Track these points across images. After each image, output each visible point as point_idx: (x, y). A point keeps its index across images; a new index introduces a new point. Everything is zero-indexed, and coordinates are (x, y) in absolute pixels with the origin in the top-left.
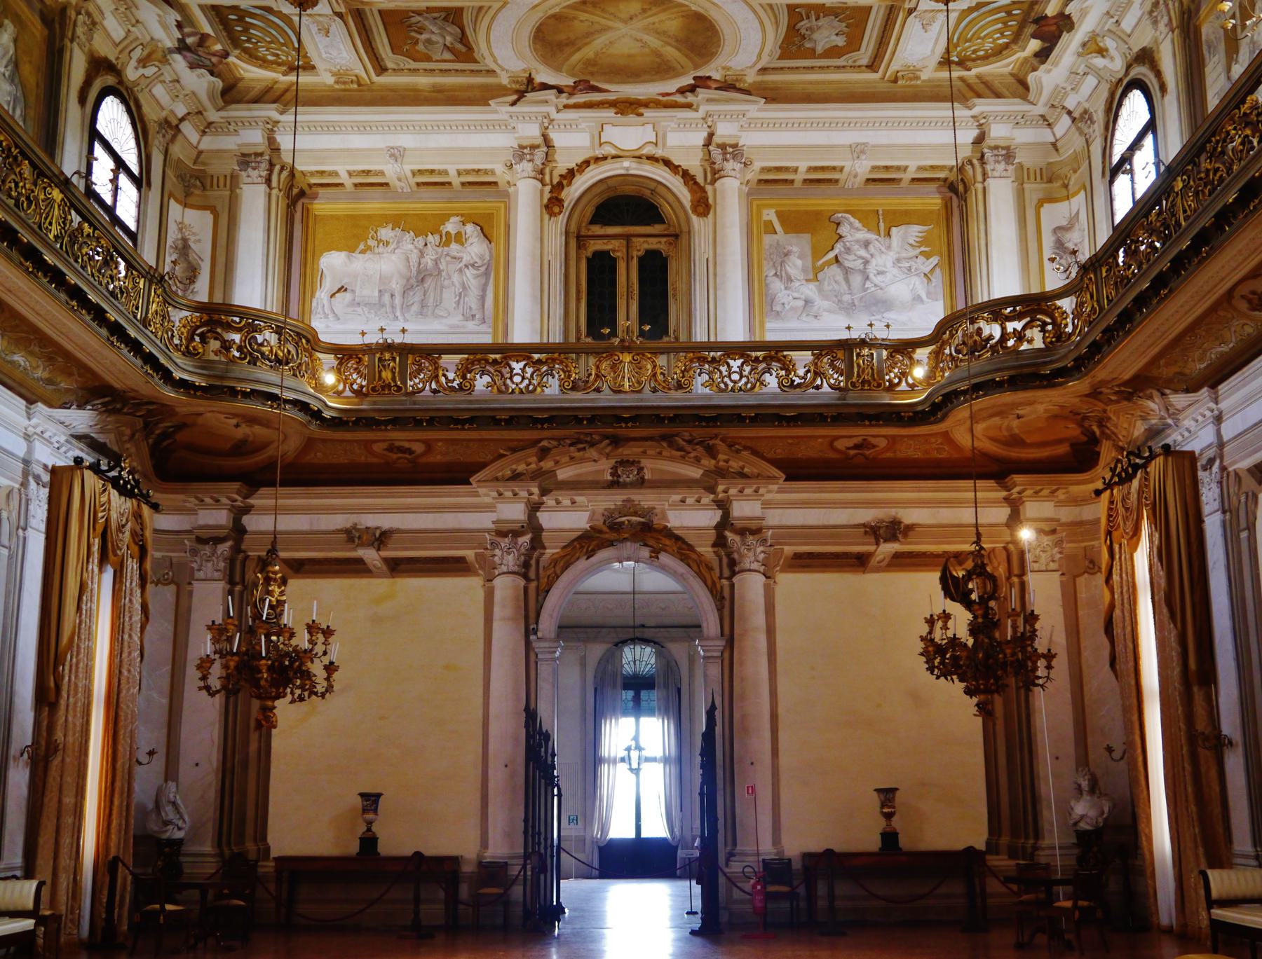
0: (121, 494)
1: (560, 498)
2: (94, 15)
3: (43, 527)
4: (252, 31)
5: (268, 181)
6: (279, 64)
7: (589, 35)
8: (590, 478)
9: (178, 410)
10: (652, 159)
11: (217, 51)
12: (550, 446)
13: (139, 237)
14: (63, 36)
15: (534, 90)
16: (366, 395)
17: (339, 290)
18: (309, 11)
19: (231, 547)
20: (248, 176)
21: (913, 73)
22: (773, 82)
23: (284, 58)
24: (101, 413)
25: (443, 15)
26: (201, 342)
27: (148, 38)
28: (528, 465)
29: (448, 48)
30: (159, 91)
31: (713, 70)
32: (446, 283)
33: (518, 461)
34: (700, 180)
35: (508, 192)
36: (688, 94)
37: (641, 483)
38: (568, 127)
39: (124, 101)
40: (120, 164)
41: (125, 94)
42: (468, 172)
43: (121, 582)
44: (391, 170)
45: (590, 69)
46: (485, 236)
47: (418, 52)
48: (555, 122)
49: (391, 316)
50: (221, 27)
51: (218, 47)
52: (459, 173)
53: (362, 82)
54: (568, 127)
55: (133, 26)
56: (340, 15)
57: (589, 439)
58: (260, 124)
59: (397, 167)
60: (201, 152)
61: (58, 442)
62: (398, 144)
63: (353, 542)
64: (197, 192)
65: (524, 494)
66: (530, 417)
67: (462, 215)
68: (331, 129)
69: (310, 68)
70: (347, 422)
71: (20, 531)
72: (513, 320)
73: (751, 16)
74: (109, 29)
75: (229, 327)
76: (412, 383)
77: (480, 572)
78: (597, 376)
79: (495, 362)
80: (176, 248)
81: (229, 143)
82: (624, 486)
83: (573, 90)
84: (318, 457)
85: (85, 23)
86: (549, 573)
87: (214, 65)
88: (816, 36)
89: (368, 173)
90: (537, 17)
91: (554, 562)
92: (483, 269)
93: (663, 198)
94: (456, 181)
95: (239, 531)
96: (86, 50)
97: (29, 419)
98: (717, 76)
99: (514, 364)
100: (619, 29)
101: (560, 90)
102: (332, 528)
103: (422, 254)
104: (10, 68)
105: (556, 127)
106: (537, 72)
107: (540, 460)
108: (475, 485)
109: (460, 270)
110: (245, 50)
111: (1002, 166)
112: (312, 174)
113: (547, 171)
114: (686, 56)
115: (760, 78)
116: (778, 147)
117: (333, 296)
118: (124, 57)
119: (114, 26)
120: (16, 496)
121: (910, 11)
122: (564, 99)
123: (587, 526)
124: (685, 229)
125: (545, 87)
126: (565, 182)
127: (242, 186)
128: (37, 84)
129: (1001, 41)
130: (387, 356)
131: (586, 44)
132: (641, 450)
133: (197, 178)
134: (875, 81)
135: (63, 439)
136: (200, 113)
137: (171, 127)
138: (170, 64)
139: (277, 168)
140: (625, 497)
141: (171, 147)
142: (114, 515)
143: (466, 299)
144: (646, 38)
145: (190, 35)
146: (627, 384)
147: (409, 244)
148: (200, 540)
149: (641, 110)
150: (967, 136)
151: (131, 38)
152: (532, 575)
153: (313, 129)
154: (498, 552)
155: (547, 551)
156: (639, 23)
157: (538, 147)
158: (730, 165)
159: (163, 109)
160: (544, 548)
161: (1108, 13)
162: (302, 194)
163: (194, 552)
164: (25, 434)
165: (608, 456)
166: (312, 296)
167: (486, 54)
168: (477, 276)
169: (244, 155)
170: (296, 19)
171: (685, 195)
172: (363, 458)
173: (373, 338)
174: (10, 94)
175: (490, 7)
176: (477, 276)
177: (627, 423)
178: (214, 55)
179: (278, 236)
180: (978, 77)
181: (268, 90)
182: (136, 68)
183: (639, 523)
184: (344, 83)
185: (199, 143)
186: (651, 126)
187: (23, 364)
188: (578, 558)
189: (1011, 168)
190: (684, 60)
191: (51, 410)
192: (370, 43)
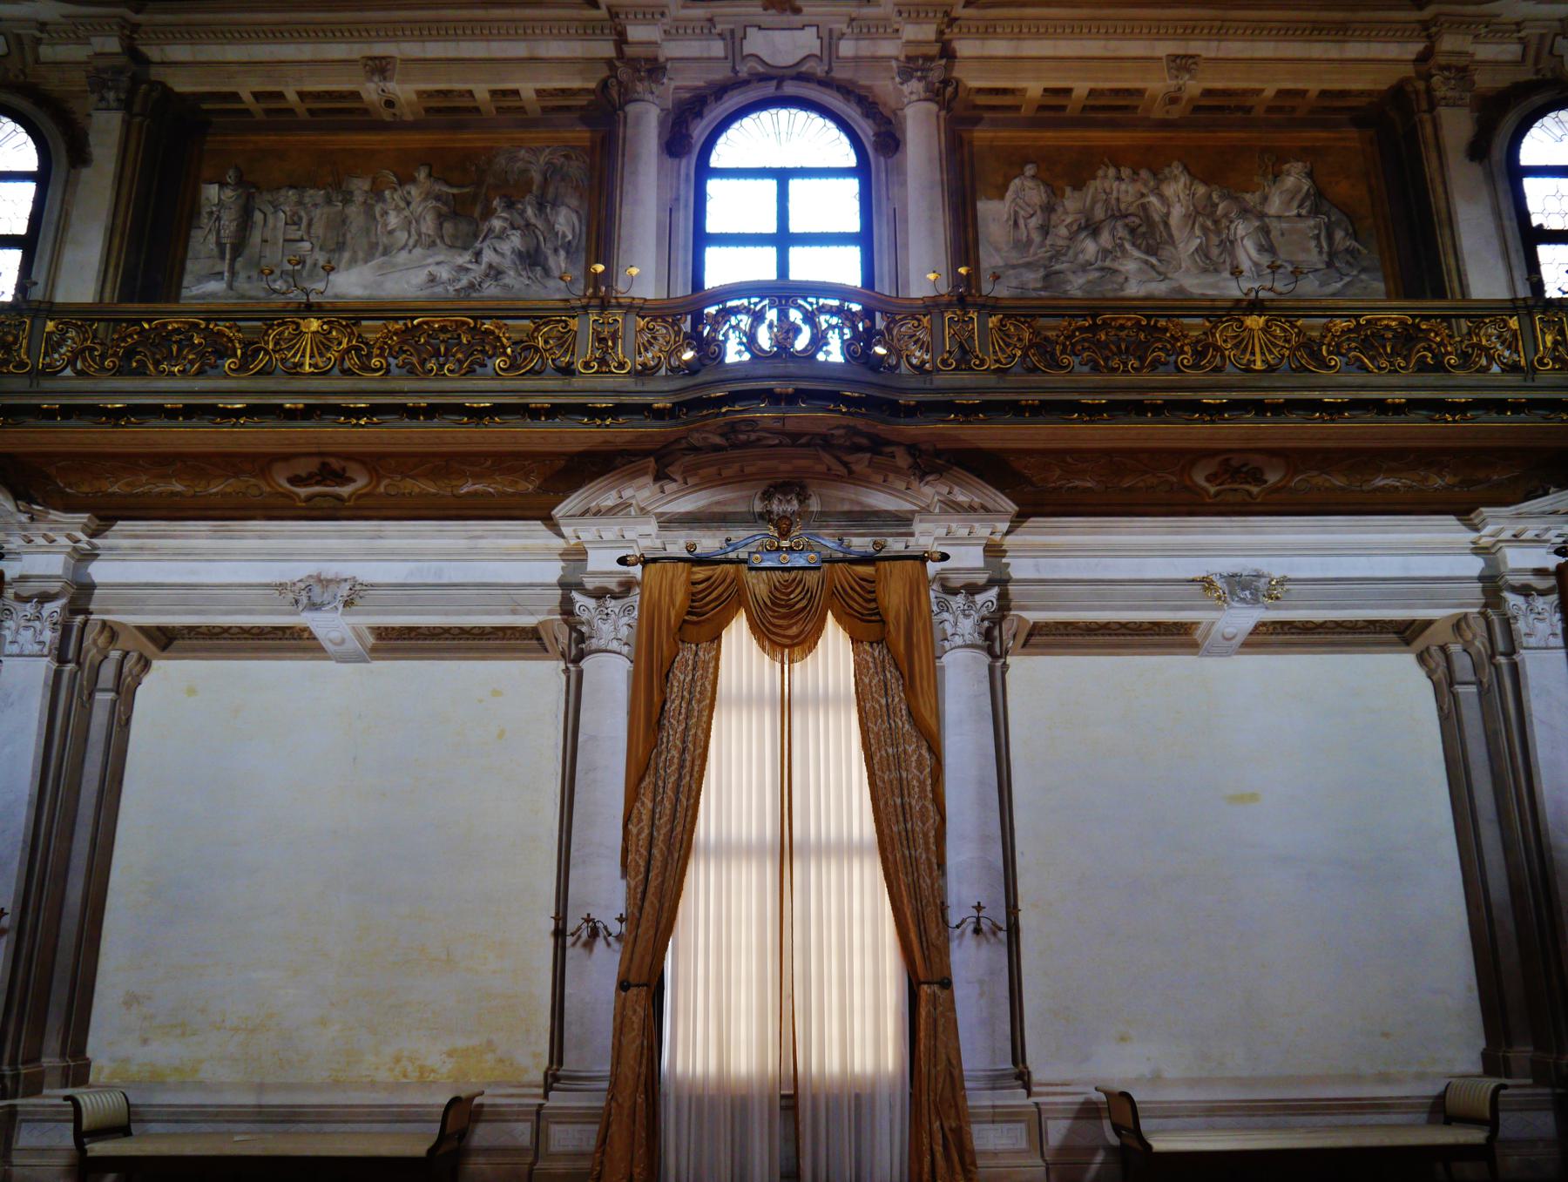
27: (1557, 24)
55: (1519, 31)
71: (1502, 660)
97: (1477, 530)
104: (1308, 203)
120: (1479, 627)
187: (1398, 484)
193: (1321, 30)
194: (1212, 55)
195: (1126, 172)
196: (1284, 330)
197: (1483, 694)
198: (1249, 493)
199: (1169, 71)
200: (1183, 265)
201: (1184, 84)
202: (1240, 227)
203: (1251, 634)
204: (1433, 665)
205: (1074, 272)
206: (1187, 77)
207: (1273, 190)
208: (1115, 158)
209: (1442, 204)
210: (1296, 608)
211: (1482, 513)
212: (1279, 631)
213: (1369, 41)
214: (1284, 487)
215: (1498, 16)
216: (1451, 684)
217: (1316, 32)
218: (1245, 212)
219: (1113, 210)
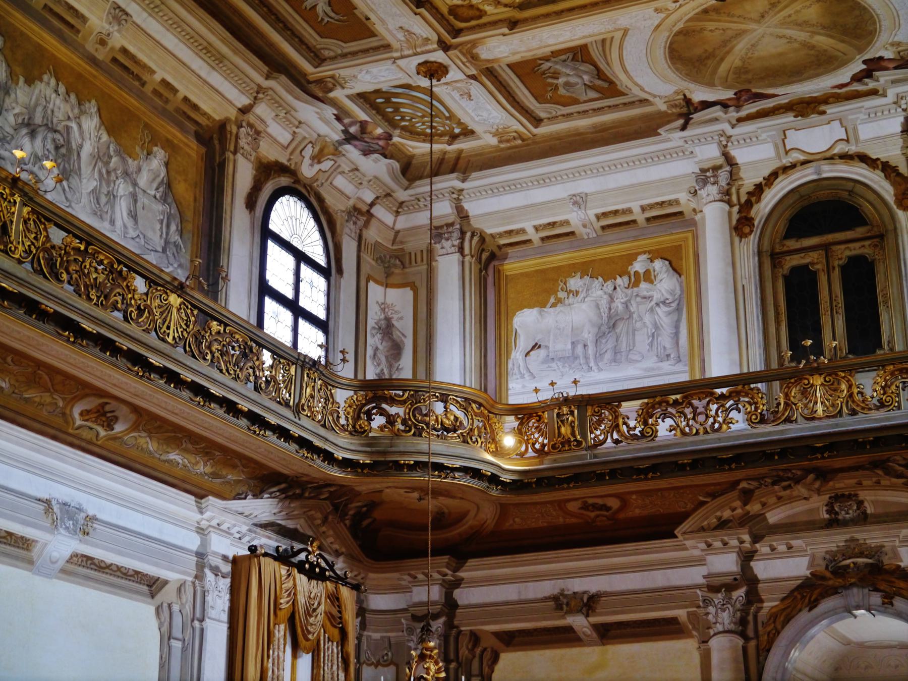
0: (310, 578)
1: (774, 544)
2: (256, 125)
3: (225, 617)
4: (402, 110)
5: (461, 249)
6: (441, 135)
7: (726, 44)
8: (804, 518)
9: (357, 489)
10: (846, 157)
11: (380, 135)
12: (752, 487)
13: (331, 324)
14: (224, 150)
15: (697, 110)
16: (547, 454)
17: (533, 348)
18: (443, 80)
19: (445, 623)
20: (442, 248)
23: (442, 129)
24: (281, 500)
26: (367, 420)
27: (315, 136)
28: (733, 510)
29: (589, 87)
30: (340, 181)
31: (881, 49)
32: (638, 325)
33: (721, 508)
35: (693, 219)
36: (866, 80)
37: (863, 519)
38: (748, 141)
40: (300, 257)
41: (304, 191)
42: (652, 206)
43: (319, 666)
44: (575, 218)
45: (744, 77)
46: (674, 270)
47: (561, 96)
48: (733, 139)
49: (585, 367)
50: (374, 112)
51: (379, 131)
52: (643, 209)
53: (525, 137)
54: (748, 140)
55: (297, 127)
56: (473, 77)
57: (789, 475)
58: (447, 195)
59: (581, 214)
60: (398, 232)
61: (239, 532)
62: (579, 191)
63: (562, 609)
64: (397, 271)
65: (734, 542)
66: (715, 458)
67: (649, 252)
68: (513, 187)
69: (468, 133)
70: (529, 485)
71: (197, 624)
72: (709, 354)
74: (274, 134)
75: (392, 401)
76: (593, 436)
77: (695, 633)
78: (786, 404)
79: (676, 402)
80: (380, 328)
82: (845, 524)
83: (738, 101)
84: (516, 522)
85: (248, 134)
86: (769, 629)
87: (383, 148)
89: (553, 225)
90: (664, 37)
91: (774, 616)
92: (674, 305)
93: (862, 197)
94: (640, 217)
95: (450, 606)
96: (253, 158)
97: (202, 513)
98: (888, 54)
99: (695, 402)
100: (755, 30)
101: (724, 105)
102: (540, 595)
103: (612, 299)
104: (161, 189)
105: (736, 143)
107: (745, 504)
108: (680, 538)
109: (652, 310)
110: (404, 128)
112: (501, 235)
113: (734, 190)
114: (843, 41)
117: (527, 354)
118: (296, 157)
119: (279, 132)
120: (189, 590)
122: (733, 114)
123: (808, 573)
124: (890, 227)
125: (706, 105)
126: (753, 199)
128: (195, 200)
130: (565, 410)
131: (728, 52)
132: (853, 481)
133: (397, 257)
135: (244, 529)
136: (388, 195)
138: (344, 155)
139: (468, 235)
140: (848, 537)
141: (364, 232)
142: (301, 600)
143: (660, 339)
144: (789, 32)
146: (820, 408)
147: (598, 290)
148: (415, 618)
152: (750, 632)
153: (496, 191)
154: (711, 609)
155: (765, 604)
157: (720, 167)
159: (349, 198)
160: (762, 601)
162: (493, 257)
163: (411, 631)
164: (198, 528)
165: (819, 492)
166: (508, 358)
167: (630, 84)
168: (669, 313)
171: (886, 190)
172: (561, 520)
173: (546, 395)
174: (163, 213)
175: (612, 38)
176: (669, 313)
177: (822, 454)
178: (379, 138)
179: (472, 301)
181: (442, 161)
182: (312, 165)
183: (867, 565)
184: (508, 141)
185: (394, 224)
186: (838, 122)
187: (180, 461)
188: (800, 610)
190: (841, 46)
191: (225, 502)
192: (514, 98)
193: (209, 52)
194: (139, 22)
195: (62, 89)
196: (187, 315)
197: (184, 649)
198: (98, 434)
199: (107, 15)
200: (82, 200)
201: (112, 33)
202: (121, 186)
203: (67, 562)
204: (163, 620)
205: (12, 164)
206: (116, 28)
207: (145, 164)
208: (59, 72)
209: (228, 235)
210: (97, 546)
211: (209, 500)
212: (84, 564)
213: (226, 79)
214: (120, 438)
215: (296, 111)
216: (169, 639)
217: (204, 51)
218: (126, 173)
219: (48, 120)
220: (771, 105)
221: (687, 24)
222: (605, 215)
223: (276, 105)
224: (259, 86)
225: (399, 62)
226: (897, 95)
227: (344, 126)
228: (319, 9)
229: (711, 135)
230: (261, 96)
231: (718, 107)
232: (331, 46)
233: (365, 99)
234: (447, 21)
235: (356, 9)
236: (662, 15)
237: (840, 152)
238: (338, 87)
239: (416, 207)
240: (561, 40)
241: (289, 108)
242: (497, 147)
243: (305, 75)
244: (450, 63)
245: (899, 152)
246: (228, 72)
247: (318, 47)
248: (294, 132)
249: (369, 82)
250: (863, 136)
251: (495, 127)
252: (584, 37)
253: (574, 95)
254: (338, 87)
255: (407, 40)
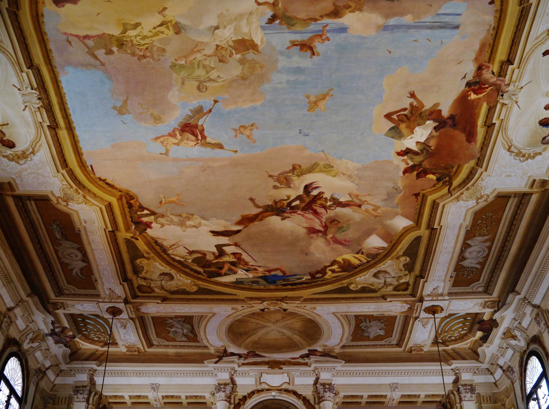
4: (88, 326)
5: (88, 401)
6: (100, 342)
7: (256, 330)
11: (70, 335)
15: (227, 356)
18: (117, 317)
20: (78, 398)
21: (420, 348)
22: (349, 352)
25: (183, 319)
27: (37, 329)
29: (185, 335)
30: (38, 354)
34: (312, 402)
36: (306, 358)
39: (20, 360)
42: (191, 397)
44: (151, 396)
45: (256, 345)
48: (237, 372)
50: (73, 324)
51: (71, 333)
52: (187, 397)
53: (140, 351)
54: (244, 374)
55: (30, 323)
56: (132, 319)
60: (55, 385)
64: (50, 406)
69: (115, 344)
73: (337, 320)
81: (70, 380)
83: (246, 356)
85: (7, 322)
87: (67, 342)
88: (369, 330)
89: (139, 397)
90: (230, 320)
94: (185, 402)
96: (5, 334)
98: (320, 349)
100: (270, 327)
106: (229, 347)
110: (84, 335)
111: (468, 395)
113: (232, 397)
114: (304, 340)
115: (342, 351)
116: (352, 385)
119: (21, 324)
121: (416, 318)
122: (242, 361)
125: (233, 354)
126: (241, 403)
127: (74, 403)
129: (462, 332)
133: (51, 398)
134: (400, 352)
136: (57, 365)
137: (42, 372)
138: (46, 341)
139: (93, 393)
145: (57, 328)
149: (282, 366)
150: (449, 379)
151: (29, 328)
156: (281, 324)
157: (228, 384)
158: (328, 394)
159: (39, 363)
161: (514, 319)
167: (204, 338)
169: (77, 387)
170: (111, 320)
178: (68, 337)
180: (453, 349)
181: (93, 354)
182: (29, 343)
184: (131, 351)
185: (54, 380)
186: (286, 374)
189: (474, 395)
190: (303, 342)
192: (146, 332)
193: (6, 277)
215: (34, 315)
217: (4, 276)
220: (260, 360)
221: (244, 318)
222: (167, 397)
223: (26, 310)
224: (22, 299)
225: (100, 304)
226: (315, 367)
227: (54, 327)
228: (74, 271)
229: (228, 368)
230: (20, 304)
231: (237, 356)
232: (72, 289)
233: (72, 318)
234: (134, 290)
235: (93, 275)
236: (234, 311)
237: (286, 388)
238: (62, 309)
239: (69, 374)
240: (183, 311)
241: (31, 313)
242: (124, 353)
243: (48, 298)
244: (125, 310)
245: (311, 393)
246: (11, 289)
247: (64, 288)
248: (28, 325)
249: (80, 310)
250: (296, 383)
251: (129, 344)
252: (194, 313)
253: (175, 337)
254: (62, 309)
255: (110, 295)
